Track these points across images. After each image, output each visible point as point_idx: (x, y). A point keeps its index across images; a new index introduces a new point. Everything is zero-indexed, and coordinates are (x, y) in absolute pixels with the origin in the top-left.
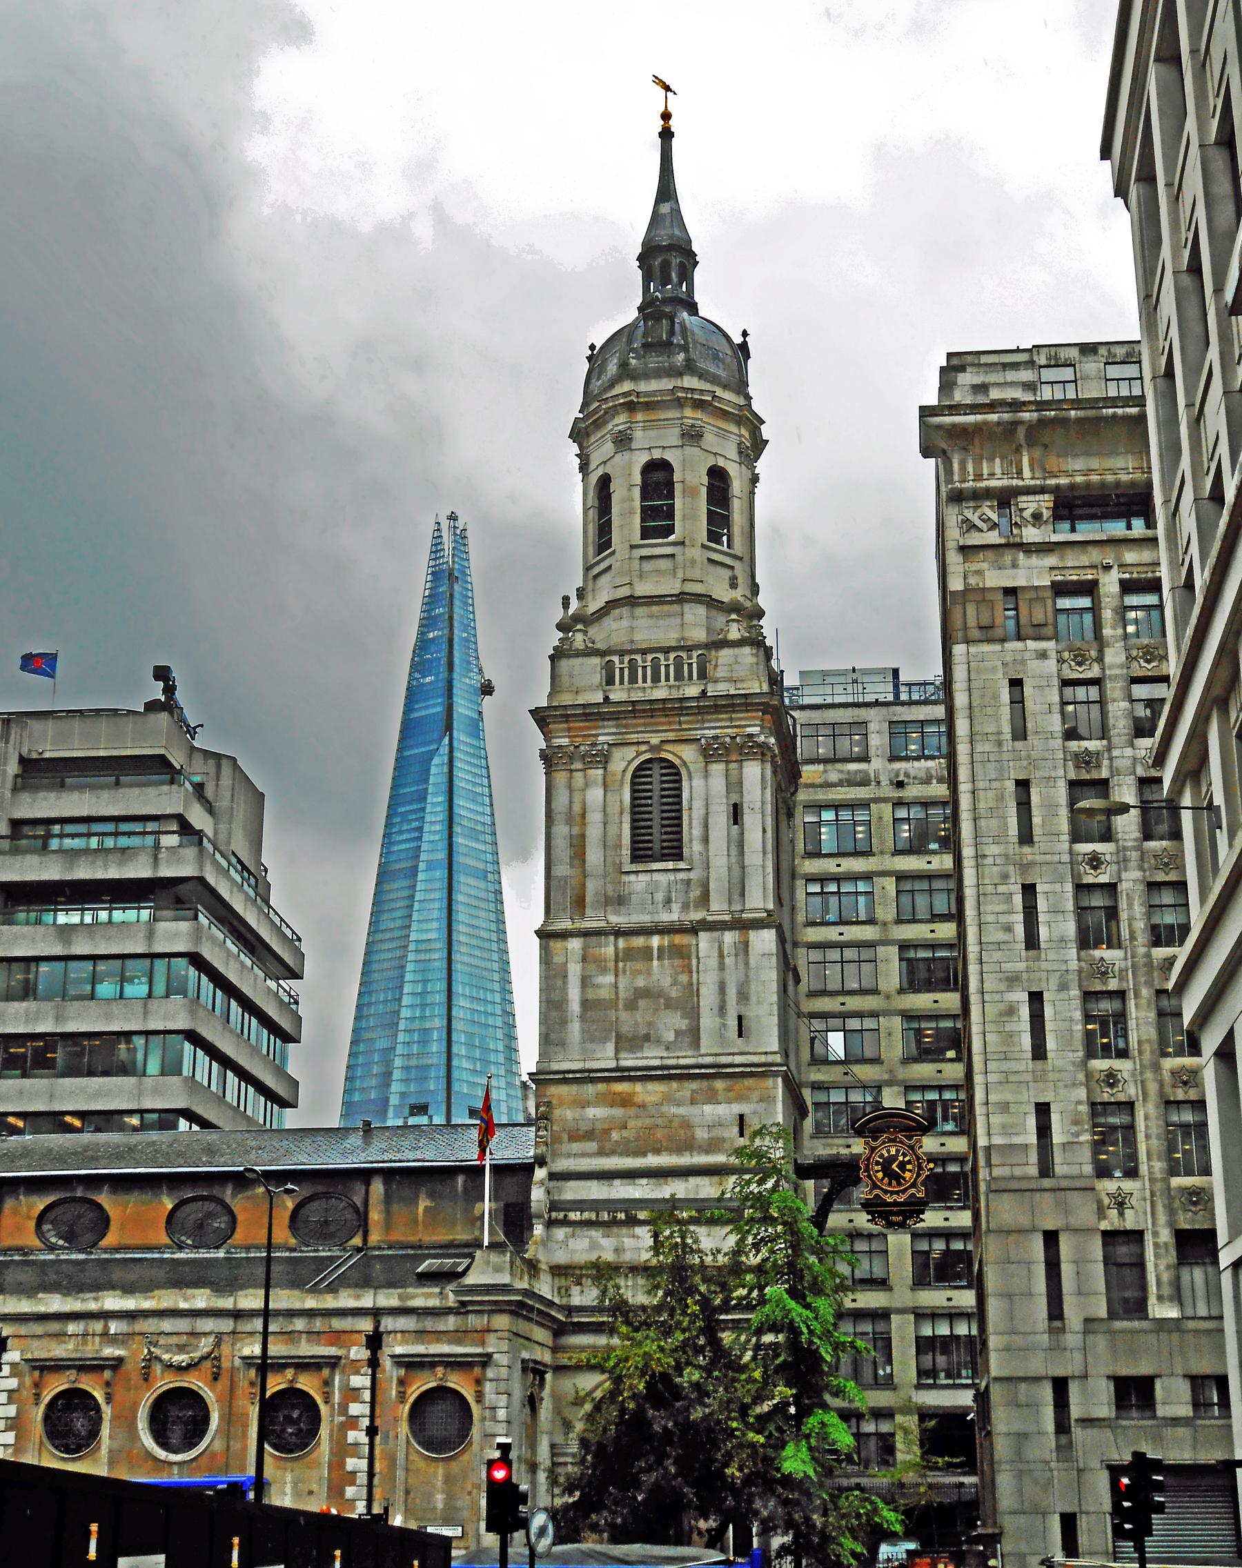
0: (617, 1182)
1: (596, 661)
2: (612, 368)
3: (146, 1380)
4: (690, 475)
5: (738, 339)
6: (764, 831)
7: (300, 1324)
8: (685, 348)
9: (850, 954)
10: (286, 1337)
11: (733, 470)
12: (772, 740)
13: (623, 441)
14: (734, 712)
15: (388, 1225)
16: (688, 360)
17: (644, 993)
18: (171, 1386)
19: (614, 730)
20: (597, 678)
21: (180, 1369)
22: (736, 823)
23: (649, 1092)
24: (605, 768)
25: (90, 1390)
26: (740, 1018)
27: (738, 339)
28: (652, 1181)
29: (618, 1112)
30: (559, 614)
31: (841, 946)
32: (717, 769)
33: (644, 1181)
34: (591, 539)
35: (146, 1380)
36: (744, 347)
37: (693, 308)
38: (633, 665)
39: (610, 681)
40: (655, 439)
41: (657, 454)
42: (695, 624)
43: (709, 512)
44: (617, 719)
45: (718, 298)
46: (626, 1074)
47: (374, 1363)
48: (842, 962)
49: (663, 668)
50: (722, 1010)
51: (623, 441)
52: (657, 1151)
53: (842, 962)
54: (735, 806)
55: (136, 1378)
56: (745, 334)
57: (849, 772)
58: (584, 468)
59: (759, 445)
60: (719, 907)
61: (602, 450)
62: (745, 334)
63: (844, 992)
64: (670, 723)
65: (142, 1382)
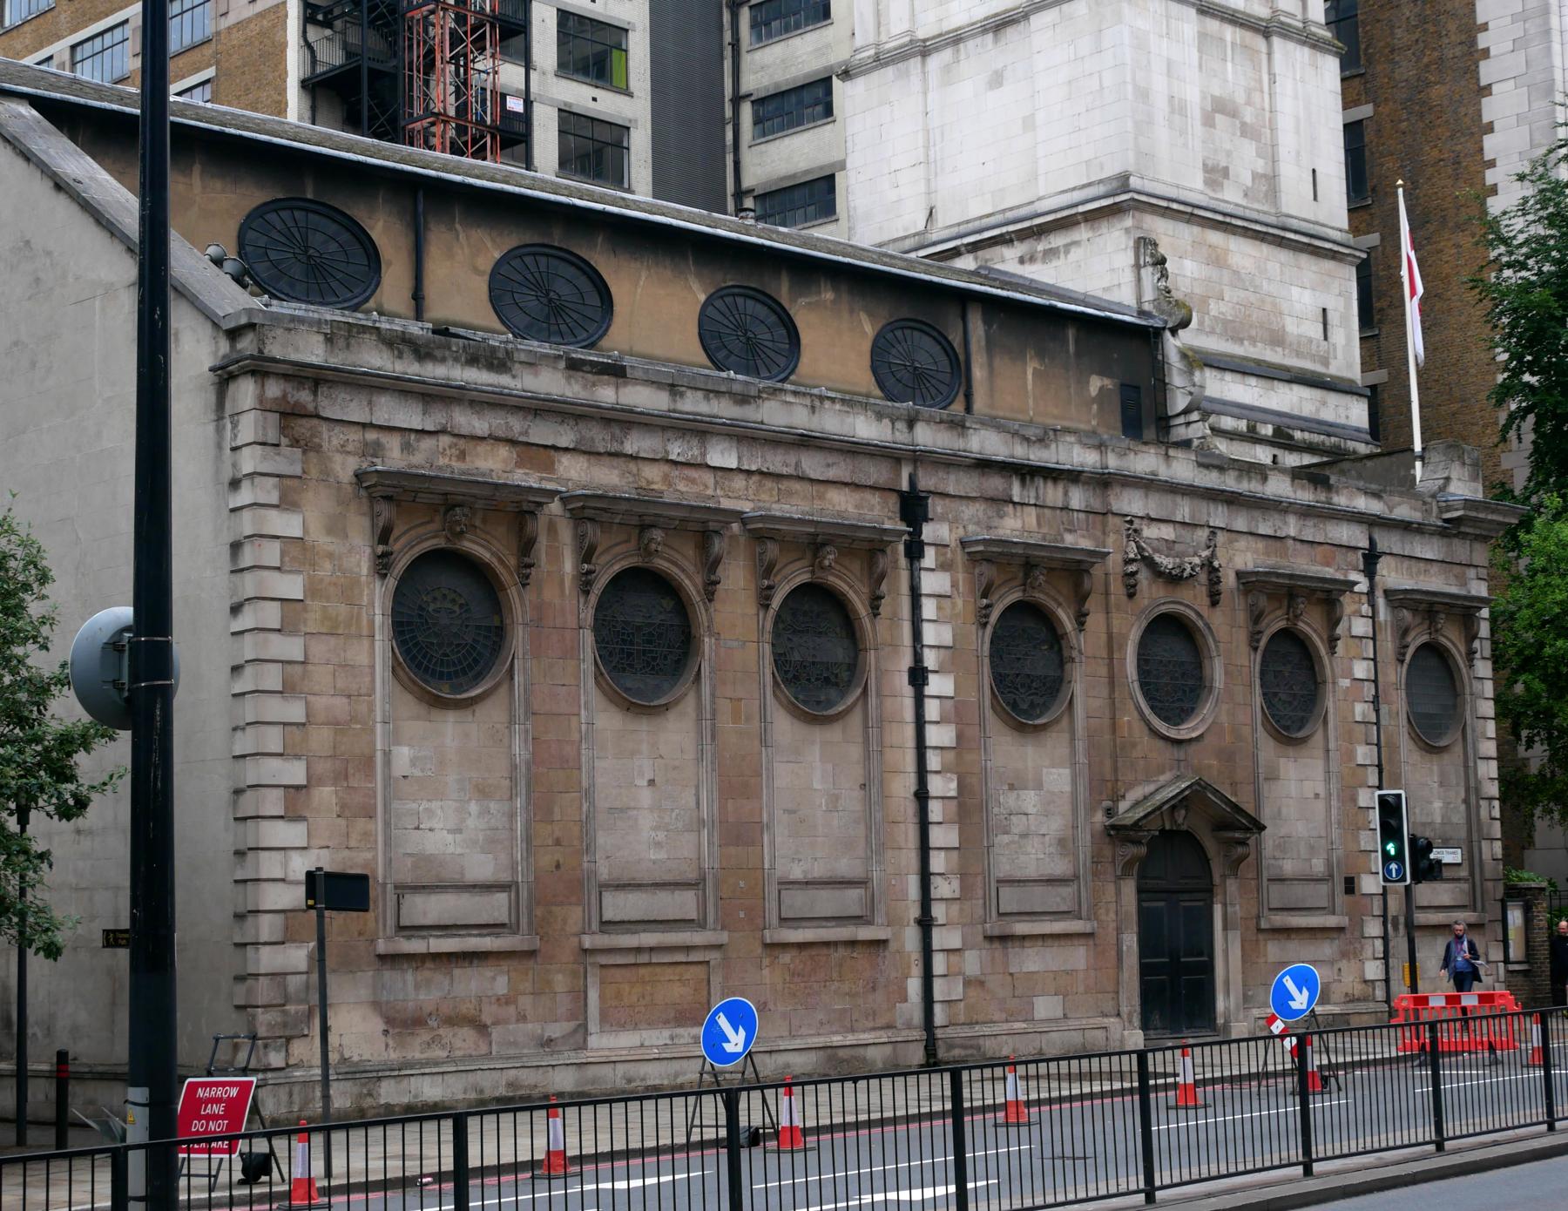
0: (1228, 376)
3: (1131, 596)
7: (1292, 527)
10: (1278, 544)
15: (991, 392)
18: (1164, 609)
21: (1174, 579)
23: (1243, 253)
25: (1052, 605)
28: (1262, 382)
29: (1213, 272)
33: (1253, 381)
35: (1131, 596)
46: (1228, 220)
47: (1371, 593)
52: (1253, 341)
55: (1117, 588)
65: (1125, 598)
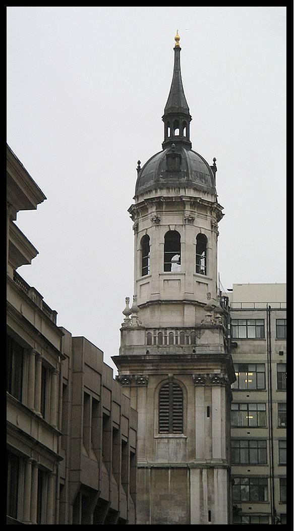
1: (143, 332)
2: (151, 183)
4: (188, 240)
5: (211, 164)
6: (222, 420)
8: (187, 174)
9: (253, 445)
11: (208, 234)
12: (226, 376)
13: (157, 221)
14: (208, 362)
16: (188, 180)
17: (163, 497)
19: (151, 368)
20: (143, 342)
22: (208, 416)
24: (147, 387)
26: (210, 512)
27: (211, 164)
30: (123, 307)
31: (249, 440)
32: (200, 391)
34: (138, 267)
36: (214, 168)
37: (189, 145)
38: (160, 335)
39: (149, 343)
40: (171, 221)
41: (172, 229)
42: (190, 317)
43: (197, 255)
44: (153, 363)
45: (203, 140)
48: (249, 448)
49: (175, 338)
50: (202, 506)
51: (157, 221)
53: (249, 448)
54: (208, 408)
56: (215, 160)
57: (254, 346)
58: (136, 228)
59: (220, 216)
60: (199, 459)
61: (146, 224)
62: (215, 160)
63: (249, 464)
64: (178, 366)
